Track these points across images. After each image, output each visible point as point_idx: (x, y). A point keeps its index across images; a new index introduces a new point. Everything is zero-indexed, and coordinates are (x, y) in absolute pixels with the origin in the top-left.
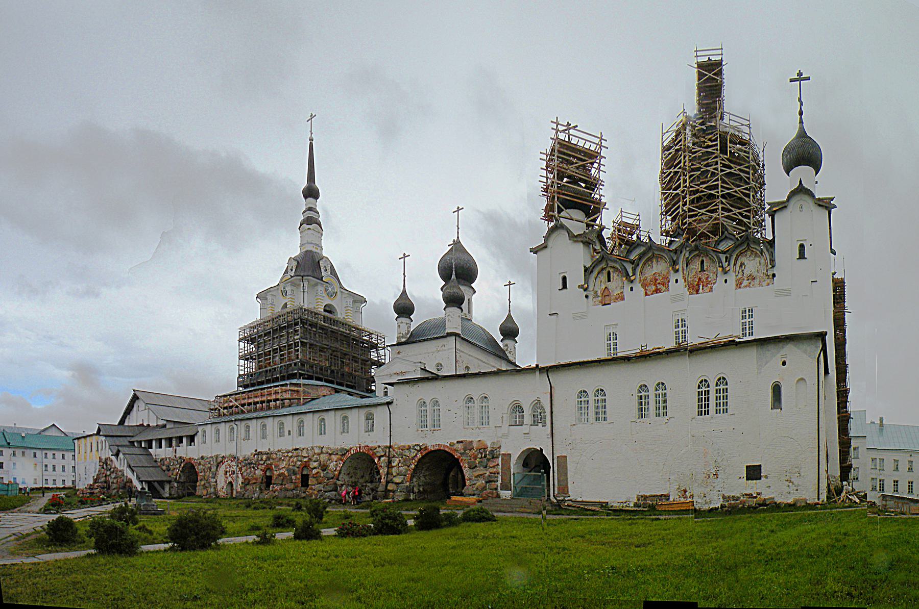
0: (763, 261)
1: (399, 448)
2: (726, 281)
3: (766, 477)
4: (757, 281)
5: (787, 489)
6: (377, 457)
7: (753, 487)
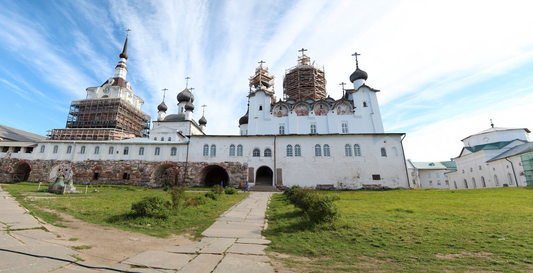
0: (348, 107)
1: (191, 163)
2: (333, 112)
3: (383, 179)
4: (346, 113)
5: (394, 184)
6: (178, 166)
7: (376, 182)
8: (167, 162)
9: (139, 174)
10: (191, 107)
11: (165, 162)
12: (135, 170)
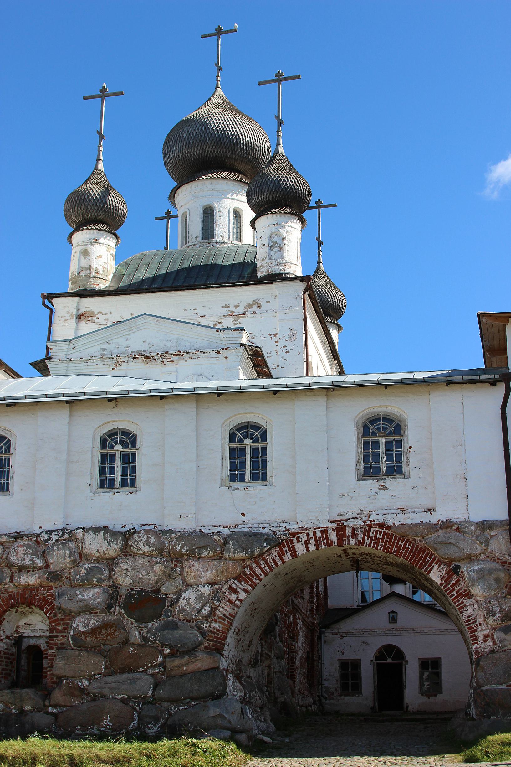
8: (341, 530)
9: (126, 643)
10: (292, 188)
11: (325, 532)
12: (89, 609)
